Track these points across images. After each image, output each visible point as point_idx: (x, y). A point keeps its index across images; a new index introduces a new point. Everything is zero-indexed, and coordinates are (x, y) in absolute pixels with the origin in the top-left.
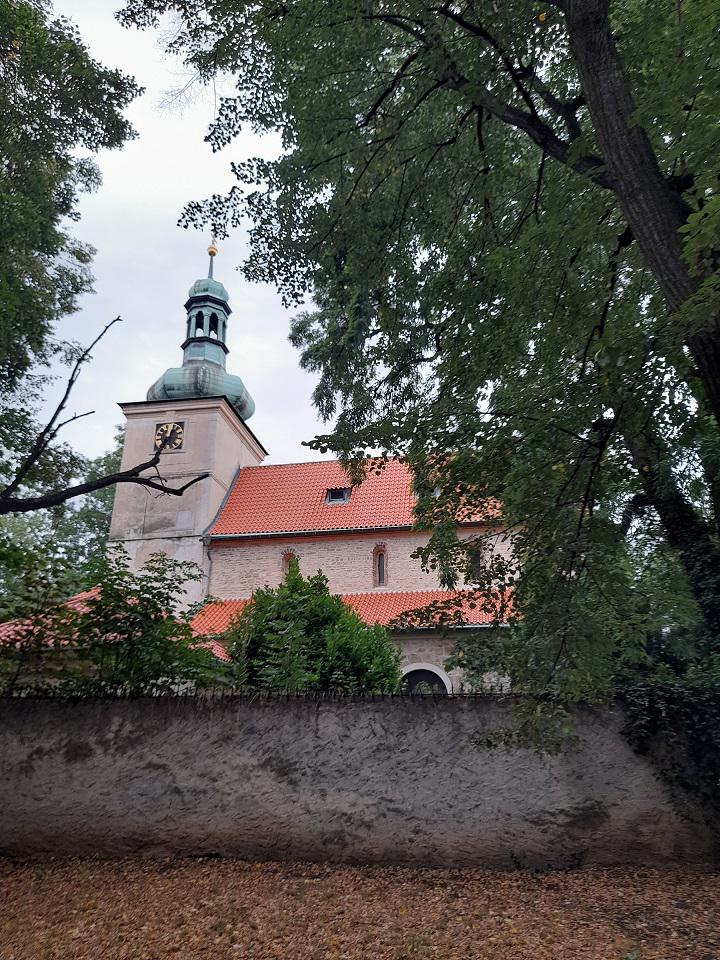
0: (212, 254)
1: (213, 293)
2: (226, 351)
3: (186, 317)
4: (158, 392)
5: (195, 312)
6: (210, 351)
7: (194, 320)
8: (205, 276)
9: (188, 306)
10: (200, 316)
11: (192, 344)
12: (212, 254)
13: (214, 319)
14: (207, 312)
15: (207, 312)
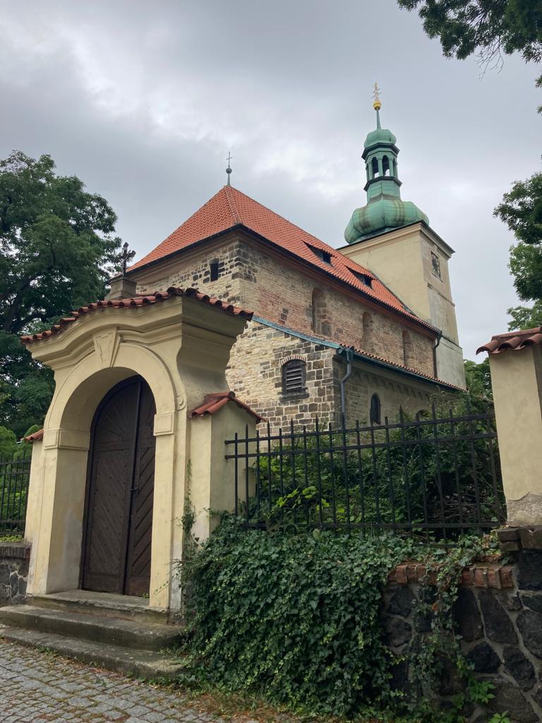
0: (377, 108)
1: (382, 139)
2: (399, 184)
3: (365, 166)
4: (353, 234)
5: (370, 159)
6: (387, 187)
7: (370, 166)
8: (376, 128)
9: (364, 156)
10: (375, 162)
11: (371, 185)
12: (377, 108)
13: (385, 159)
14: (380, 156)
15: (380, 156)
